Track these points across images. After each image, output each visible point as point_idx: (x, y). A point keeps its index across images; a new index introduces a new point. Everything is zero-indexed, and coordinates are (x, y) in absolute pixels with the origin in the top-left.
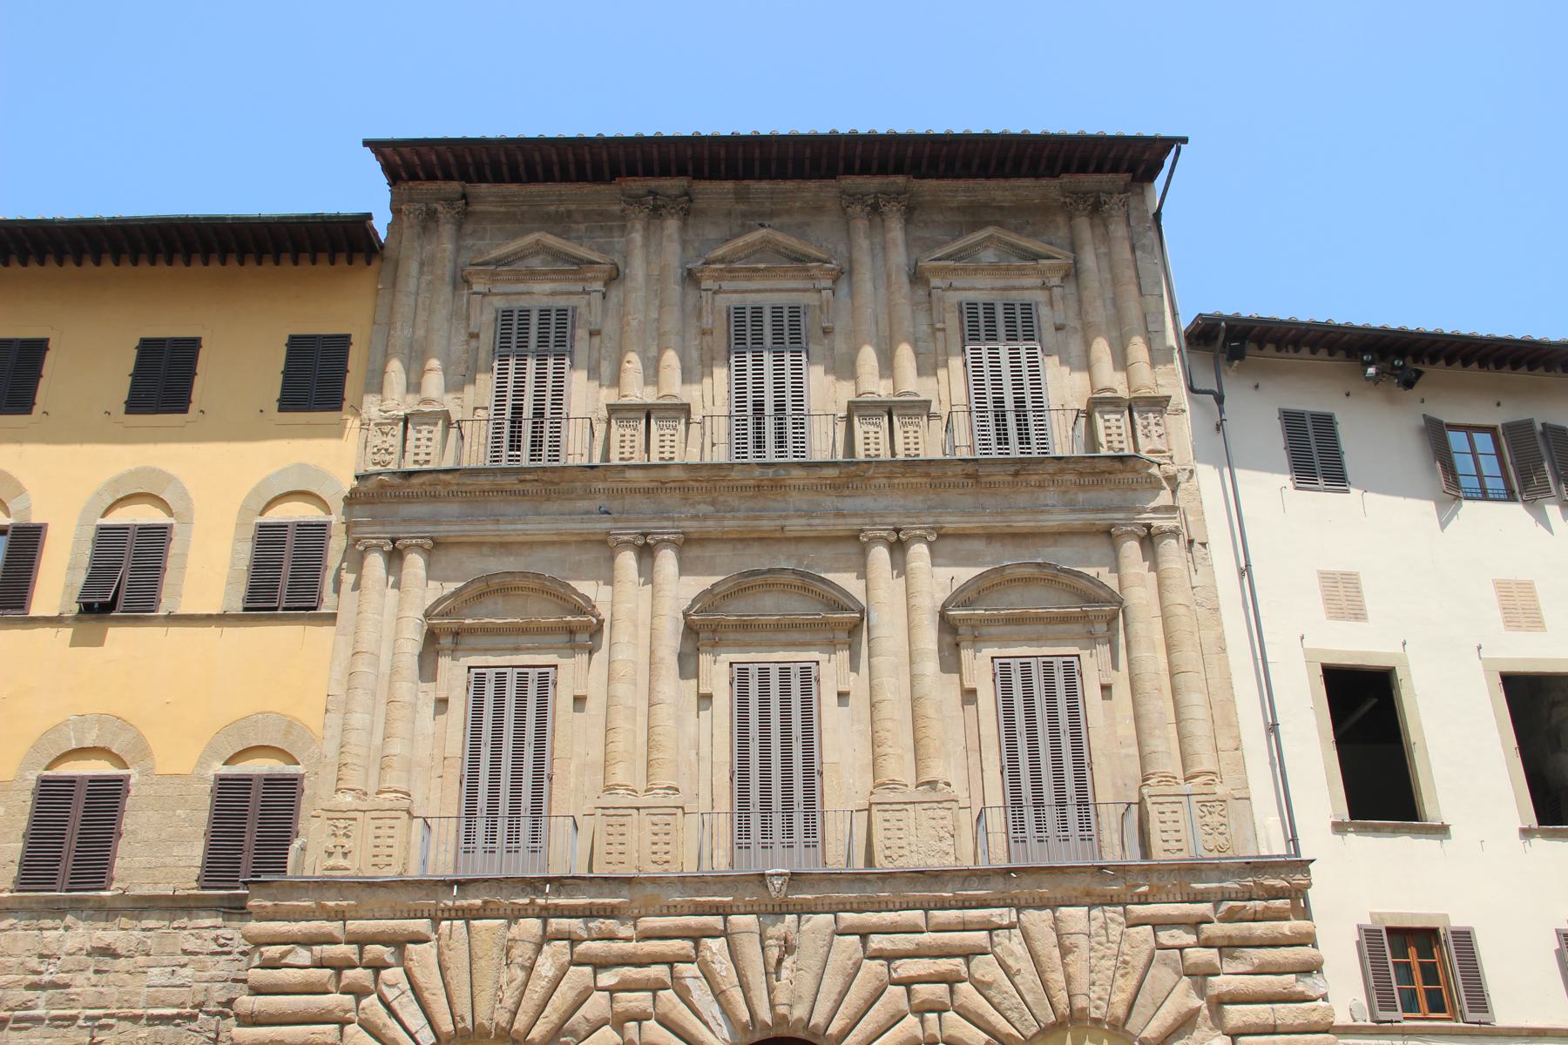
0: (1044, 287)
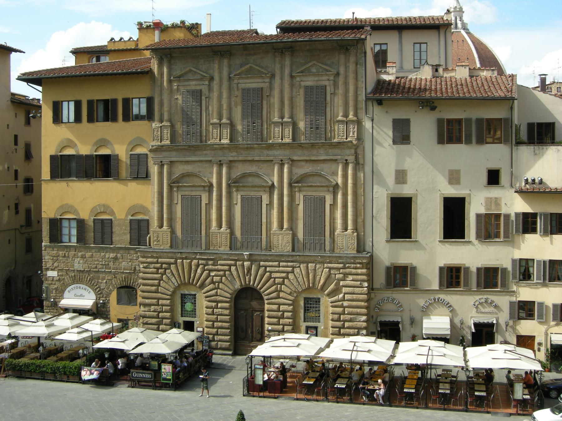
0: (328, 80)
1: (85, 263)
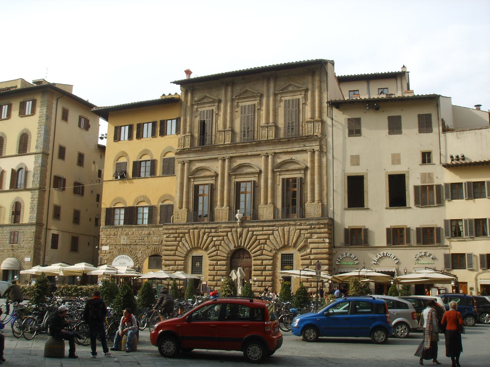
1: (128, 239)
